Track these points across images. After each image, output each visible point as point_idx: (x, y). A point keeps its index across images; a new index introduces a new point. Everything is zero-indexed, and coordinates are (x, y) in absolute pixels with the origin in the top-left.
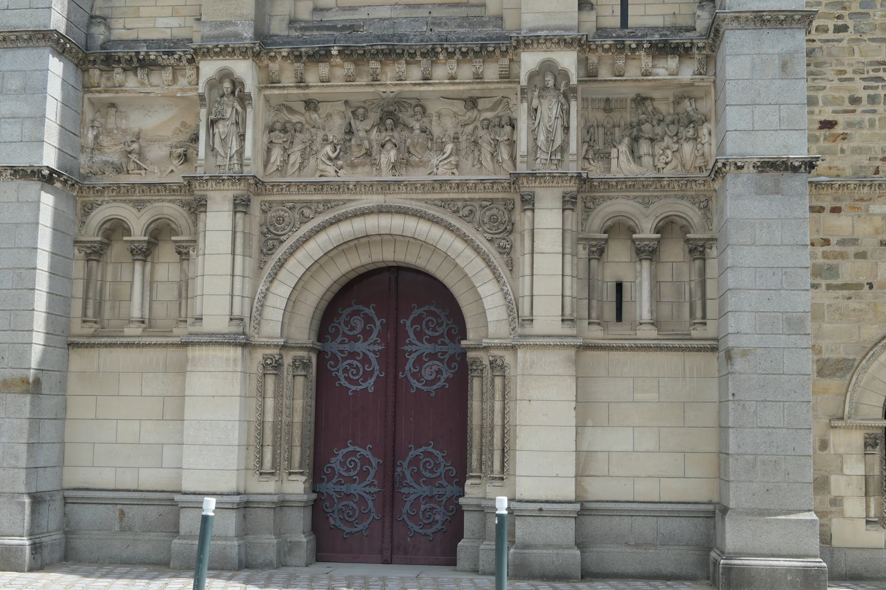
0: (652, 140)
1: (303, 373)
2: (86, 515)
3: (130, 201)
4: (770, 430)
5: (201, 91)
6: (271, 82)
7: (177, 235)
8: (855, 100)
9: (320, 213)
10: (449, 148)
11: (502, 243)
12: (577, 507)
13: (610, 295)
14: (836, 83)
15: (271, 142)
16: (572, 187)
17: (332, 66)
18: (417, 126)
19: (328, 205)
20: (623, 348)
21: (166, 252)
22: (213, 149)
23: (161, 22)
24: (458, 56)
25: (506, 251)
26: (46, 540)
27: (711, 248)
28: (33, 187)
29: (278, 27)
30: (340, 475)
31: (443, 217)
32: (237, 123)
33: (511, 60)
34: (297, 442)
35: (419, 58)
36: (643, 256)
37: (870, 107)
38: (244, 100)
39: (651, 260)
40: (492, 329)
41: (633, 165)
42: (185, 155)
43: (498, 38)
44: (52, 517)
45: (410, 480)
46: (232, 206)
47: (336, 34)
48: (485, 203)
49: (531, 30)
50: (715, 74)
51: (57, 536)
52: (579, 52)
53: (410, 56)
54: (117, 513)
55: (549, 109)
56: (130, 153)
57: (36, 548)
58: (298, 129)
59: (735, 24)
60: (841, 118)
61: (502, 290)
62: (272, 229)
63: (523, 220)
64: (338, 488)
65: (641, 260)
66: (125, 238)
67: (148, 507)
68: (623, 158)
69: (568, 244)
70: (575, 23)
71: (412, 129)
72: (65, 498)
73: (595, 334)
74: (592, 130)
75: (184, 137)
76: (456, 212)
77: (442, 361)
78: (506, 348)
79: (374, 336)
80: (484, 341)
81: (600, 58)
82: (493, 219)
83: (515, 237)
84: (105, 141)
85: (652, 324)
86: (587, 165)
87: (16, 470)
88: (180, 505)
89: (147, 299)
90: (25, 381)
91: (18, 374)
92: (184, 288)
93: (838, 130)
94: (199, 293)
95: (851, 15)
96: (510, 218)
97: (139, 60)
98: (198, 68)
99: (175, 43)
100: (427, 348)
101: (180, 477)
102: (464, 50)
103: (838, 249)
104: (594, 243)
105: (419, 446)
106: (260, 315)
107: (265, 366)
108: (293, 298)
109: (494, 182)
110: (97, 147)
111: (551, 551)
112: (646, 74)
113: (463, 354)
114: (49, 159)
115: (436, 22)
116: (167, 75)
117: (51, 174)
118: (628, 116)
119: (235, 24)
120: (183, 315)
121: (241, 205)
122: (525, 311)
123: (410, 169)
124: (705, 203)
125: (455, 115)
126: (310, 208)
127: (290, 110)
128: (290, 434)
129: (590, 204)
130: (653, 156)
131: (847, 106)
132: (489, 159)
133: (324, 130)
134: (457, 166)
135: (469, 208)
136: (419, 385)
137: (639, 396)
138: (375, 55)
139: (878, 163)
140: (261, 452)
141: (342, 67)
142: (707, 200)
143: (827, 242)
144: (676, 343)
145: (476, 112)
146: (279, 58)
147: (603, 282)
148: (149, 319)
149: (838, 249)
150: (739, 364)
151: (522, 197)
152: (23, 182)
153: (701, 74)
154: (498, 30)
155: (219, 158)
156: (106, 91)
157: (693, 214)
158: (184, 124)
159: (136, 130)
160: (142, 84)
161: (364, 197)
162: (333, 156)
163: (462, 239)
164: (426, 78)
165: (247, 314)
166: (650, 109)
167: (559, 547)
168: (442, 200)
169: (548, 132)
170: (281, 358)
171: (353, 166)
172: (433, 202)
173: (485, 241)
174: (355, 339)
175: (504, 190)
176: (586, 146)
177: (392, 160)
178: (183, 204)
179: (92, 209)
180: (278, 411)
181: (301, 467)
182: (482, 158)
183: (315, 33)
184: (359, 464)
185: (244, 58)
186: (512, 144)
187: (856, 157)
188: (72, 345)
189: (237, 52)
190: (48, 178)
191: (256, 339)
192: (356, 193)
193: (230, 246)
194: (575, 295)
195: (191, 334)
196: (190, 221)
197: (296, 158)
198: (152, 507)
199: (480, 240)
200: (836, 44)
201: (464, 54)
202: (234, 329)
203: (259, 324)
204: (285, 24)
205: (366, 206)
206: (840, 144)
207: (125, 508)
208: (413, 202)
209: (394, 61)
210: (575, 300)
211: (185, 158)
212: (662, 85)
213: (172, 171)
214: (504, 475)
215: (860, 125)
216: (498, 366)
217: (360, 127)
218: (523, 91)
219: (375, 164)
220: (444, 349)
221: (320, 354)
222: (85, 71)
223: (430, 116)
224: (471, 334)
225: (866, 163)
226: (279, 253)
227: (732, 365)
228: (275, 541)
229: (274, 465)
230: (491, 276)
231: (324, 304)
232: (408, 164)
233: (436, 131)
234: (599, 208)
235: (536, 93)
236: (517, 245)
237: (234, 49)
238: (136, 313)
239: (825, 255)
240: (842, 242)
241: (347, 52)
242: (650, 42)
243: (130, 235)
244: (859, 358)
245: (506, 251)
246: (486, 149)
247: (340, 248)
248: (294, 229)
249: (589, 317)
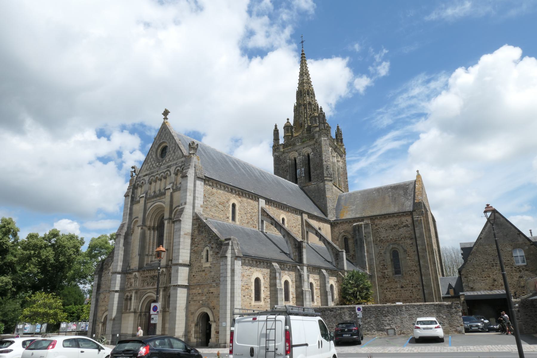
93: (195, 276)
121: (136, 293)
180: (140, 322)
188: (122, 313)
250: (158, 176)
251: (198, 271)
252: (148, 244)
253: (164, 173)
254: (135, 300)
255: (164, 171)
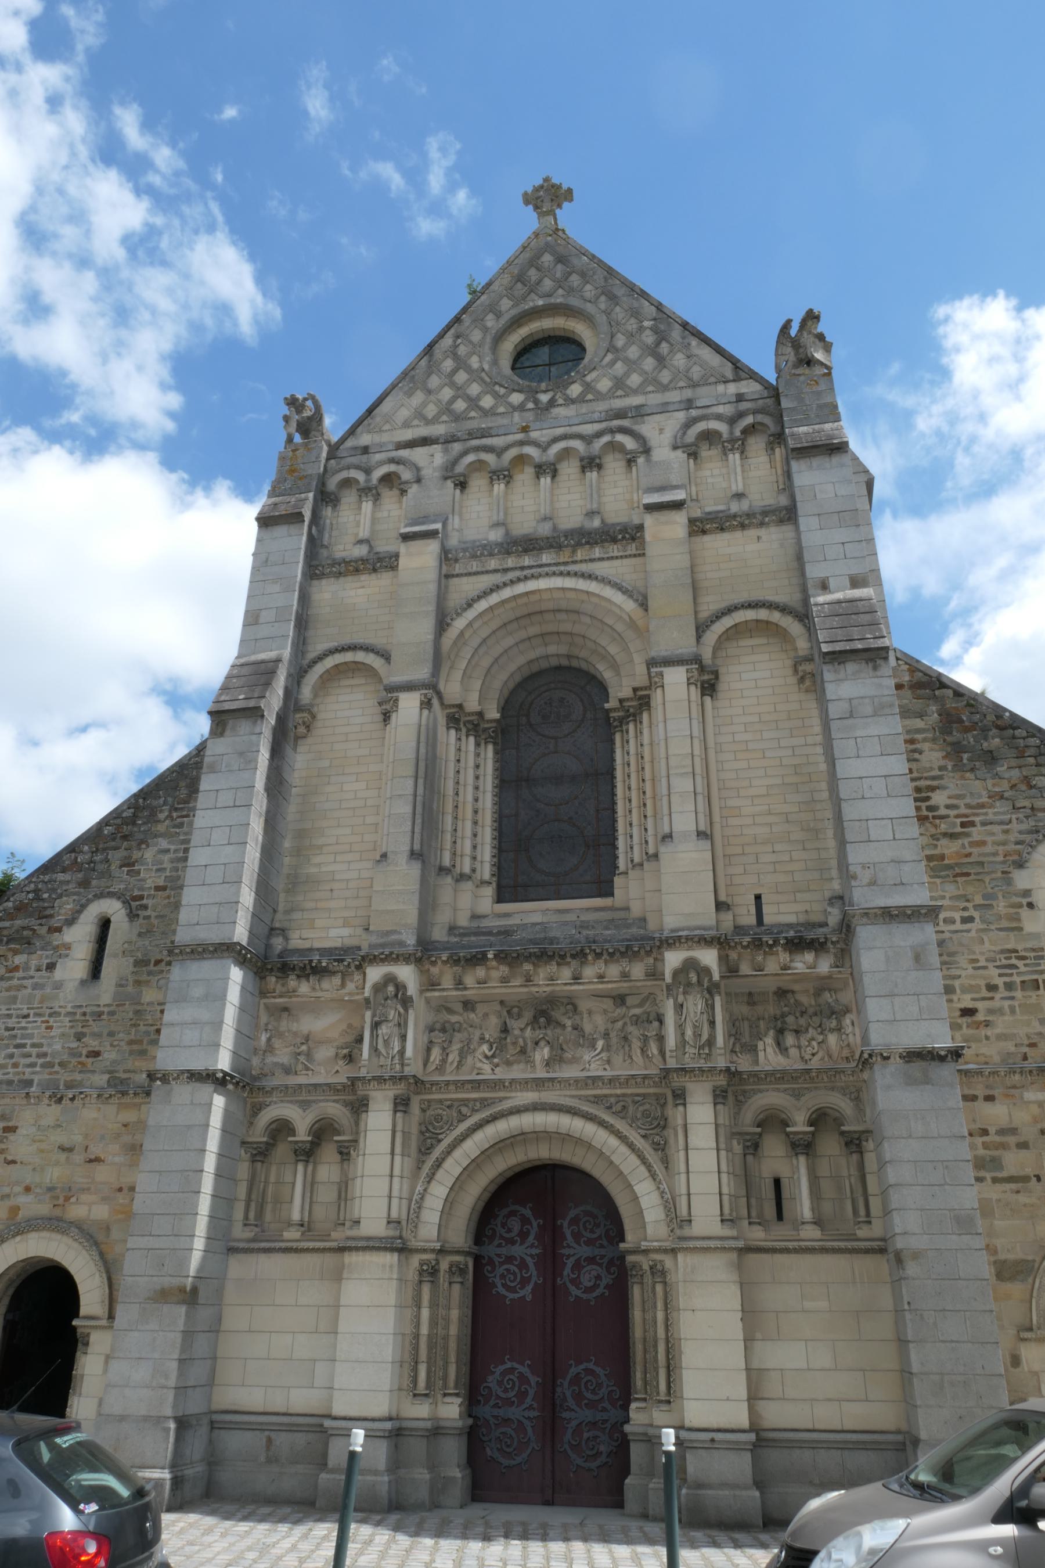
0: (797, 1032)
1: (460, 1280)
2: (234, 1442)
3: (297, 1101)
4: (953, 1345)
5: (366, 994)
6: (431, 984)
7: (339, 1135)
8: (992, 988)
9: (477, 1111)
10: (600, 1044)
11: (657, 1139)
12: (752, 1437)
13: (769, 1192)
14: (970, 971)
15: (431, 1042)
16: (722, 1081)
17: (488, 969)
18: (569, 1023)
19: (485, 1103)
20: (786, 1251)
21: (328, 1153)
22: (376, 1050)
23: (333, 933)
24: (605, 956)
25: (661, 1148)
26: (189, 1472)
27: (867, 1141)
28: (208, 1088)
29: (439, 934)
30: (498, 1397)
31: (597, 1113)
32: (399, 1025)
33: (656, 959)
34: (453, 1358)
35: (569, 959)
36: (799, 1150)
37: (1007, 994)
38: (406, 1002)
39: (807, 1154)
40: (650, 1230)
41: (780, 1057)
42: (350, 1056)
43: (643, 938)
44: (197, 1445)
45: (571, 1402)
46: (392, 1105)
47: (492, 938)
48: (639, 1098)
49: (673, 931)
50: (851, 967)
51: (200, 1468)
52: (719, 949)
53: (561, 958)
54: (264, 1440)
55: (695, 1004)
56: (299, 1054)
57: (177, 1482)
58: (457, 1028)
59: (865, 920)
60: (980, 1005)
61: (659, 1188)
62: (430, 1128)
63: (675, 1115)
64: (496, 1412)
65: (797, 1154)
66: (290, 1139)
67: (296, 1434)
68: (769, 1050)
69: (722, 1139)
70: (714, 923)
71: (564, 1027)
72: (212, 1422)
73: (757, 1235)
74: (737, 1023)
75: (349, 1038)
76: (609, 1108)
77: (600, 1265)
78: (665, 1251)
79: (531, 1239)
80: (643, 1243)
81: (740, 955)
82: (646, 1114)
83: (669, 1133)
84: (277, 1043)
85: (815, 1223)
86: (735, 1058)
87: (165, 1391)
88: (330, 1432)
89: (308, 1200)
90: (182, 1290)
91: (176, 1282)
92: (343, 1189)
93: (980, 1017)
94: (358, 1195)
95: (976, 907)
96: (662, 1113)
97: (312, 967)
98: (365, 974)
99: (345, 951)
100: (585, 1251)
101: (330, 1399)
102: (611, 950)
103: (998, 1139)
104: (748, 1137)
105: (579, 1362)
106: (417, 1217)
107: (421, 1273)
108: (450, 1200)
109: (645, 1077)
110: (270, 1049)
111: (727, 1492)
112: (785, 968)
113: (622, 1258)
114: (224, 1062)
115: (585, 925)
116: (337, 980)
117: (224, 1077)
118: (771, 1009)
119: (400, 933)
120: (342, 1218)
121: (401, 1104)
122: (683, 1211)
123: (564, 1065)
124: (856, 1094)
125: (605, 1011)
126: (467, 1106)
127: (450, 1011)
128: (446, 1348)
129: (741, 1098)
130: (799, 1047)
131: (985, 993)
132: (639, 1054)
133: (481, 1028)
134: (609, 1062)
135: (622, 1103)
136: (578, 1293)
137: (809, 1305)
138: (528, 957)
139: (1026, 1049)
140: (415, 1370)
141: (497, 969)
142: (859, 1090)
143: (985, 1132)
144: (842, 1244)
145: (624, 1009)
146: (439, 963)
147: (761, 1178)
148: (309, 1222)
149: (998, 1139)
150: (912, 1269)
151: (673, 1092)
152: (198, 1085)
153: (837, 967)
154: (642, 932)
155: (382, 1059)
156: (281, 996)
157: (844, 1105)
158: (350, 1026)
159: (306, 1032)
160: (314, 989)
161: (519, 1094)
162: (489, 1054)
163: (616, 1135)
164: (576, 978)
165: (404, 1216)
166: (792, 1001)
167: (735, 1486)
168: (595, 1096)
169: (695, 1027)
170: (438, 1263)
171: (508, 1063)
172: (587, 1099)
173: (639, 1137)
174: (512, 1242)
175: (656, 1085)
176: (732, 1040)
177: (546, 1057)
178: (346, 1104)
179: (260, 1110)
180: (433, 1322)
181: (456, 1387)
182: (633, 1053)
183: (473, 938)
184: (517, 1384)
185: (407, 964)
186: (661, 1039)
187: (1002, 1044)
188: (231, 1250)
189: (401, 958)
190: (219, 1081)
191: (413, 1244)
192: (511, 1091)
193: (389, 1145)
194: (733, 1193)
195: (348, 1238)
196: (352, 1121)
197: (453, 1057)
198: (300, 1434)
199: (634, 1137)
200: (965, 934)
201: (611, 955)
202: (391, 1233)
203: (416, 1227)
204: (445, 931)
205: (521, 1103)
206: (983, 1032)
207: (273, 1435)
208: (567, 1099)
209: (546, 963)
210: (733, 1199)
211: (350, 1058)
212: (801, 978)
213: (337, 1071)
214: (671, 1397)
215: (1000, 1011)
216: (659, 1273)
217: (515, 1025)
218: (668, 987)
219: (530, 1062)
220: (603, 1252)
221: (478, 1259)
222: (263, 978)
223: (581, 1014)
224: (629, 1237)
225: (1013, 1049)
226: (437, 1152)
227: (903, 1269)
228: (428, 1476)
229: (429, 1385)
230: (647, 1174)
231: (481, 1205)
232: (561, 1060)
233: (588, 1028)
234: (750, 1101)
235: (681, 990)
236: (672, 1140)
237: (398, 956)
238: (296, 1216)
239: (986, 1146)
240: (1001, 1132)
241: (502, 955)
242: (786, 938)
243: (294, 1136)
244: (1038, 1259)
245: (661, 1148)
246: (636, 1045)
247: (497, 1147)
248: (451, 1127)
249: (749, 1217)
250: (529, 450)
251: (1009, 986)
252: (449, 808)
253: (587, 439)
254: (398, 1159)
255: (589, 429)
